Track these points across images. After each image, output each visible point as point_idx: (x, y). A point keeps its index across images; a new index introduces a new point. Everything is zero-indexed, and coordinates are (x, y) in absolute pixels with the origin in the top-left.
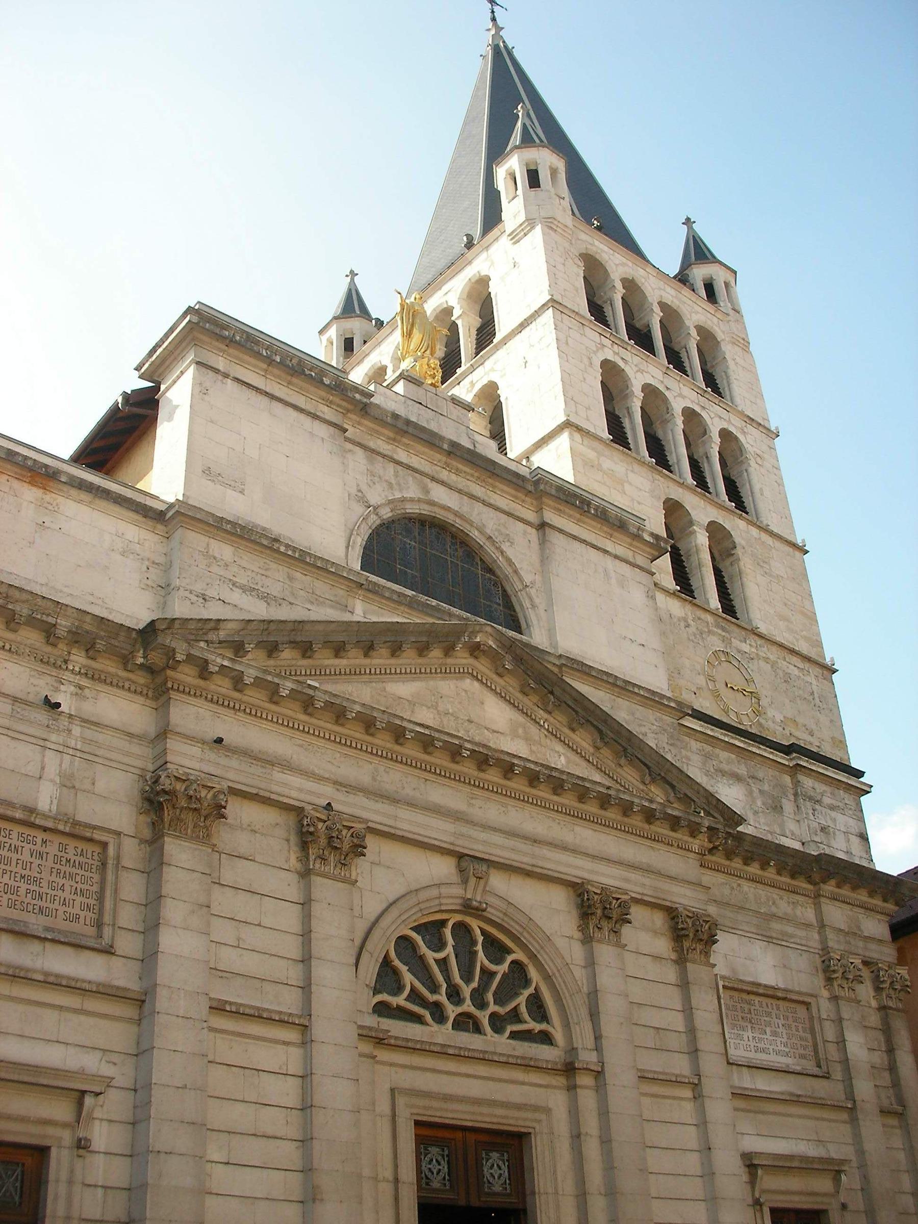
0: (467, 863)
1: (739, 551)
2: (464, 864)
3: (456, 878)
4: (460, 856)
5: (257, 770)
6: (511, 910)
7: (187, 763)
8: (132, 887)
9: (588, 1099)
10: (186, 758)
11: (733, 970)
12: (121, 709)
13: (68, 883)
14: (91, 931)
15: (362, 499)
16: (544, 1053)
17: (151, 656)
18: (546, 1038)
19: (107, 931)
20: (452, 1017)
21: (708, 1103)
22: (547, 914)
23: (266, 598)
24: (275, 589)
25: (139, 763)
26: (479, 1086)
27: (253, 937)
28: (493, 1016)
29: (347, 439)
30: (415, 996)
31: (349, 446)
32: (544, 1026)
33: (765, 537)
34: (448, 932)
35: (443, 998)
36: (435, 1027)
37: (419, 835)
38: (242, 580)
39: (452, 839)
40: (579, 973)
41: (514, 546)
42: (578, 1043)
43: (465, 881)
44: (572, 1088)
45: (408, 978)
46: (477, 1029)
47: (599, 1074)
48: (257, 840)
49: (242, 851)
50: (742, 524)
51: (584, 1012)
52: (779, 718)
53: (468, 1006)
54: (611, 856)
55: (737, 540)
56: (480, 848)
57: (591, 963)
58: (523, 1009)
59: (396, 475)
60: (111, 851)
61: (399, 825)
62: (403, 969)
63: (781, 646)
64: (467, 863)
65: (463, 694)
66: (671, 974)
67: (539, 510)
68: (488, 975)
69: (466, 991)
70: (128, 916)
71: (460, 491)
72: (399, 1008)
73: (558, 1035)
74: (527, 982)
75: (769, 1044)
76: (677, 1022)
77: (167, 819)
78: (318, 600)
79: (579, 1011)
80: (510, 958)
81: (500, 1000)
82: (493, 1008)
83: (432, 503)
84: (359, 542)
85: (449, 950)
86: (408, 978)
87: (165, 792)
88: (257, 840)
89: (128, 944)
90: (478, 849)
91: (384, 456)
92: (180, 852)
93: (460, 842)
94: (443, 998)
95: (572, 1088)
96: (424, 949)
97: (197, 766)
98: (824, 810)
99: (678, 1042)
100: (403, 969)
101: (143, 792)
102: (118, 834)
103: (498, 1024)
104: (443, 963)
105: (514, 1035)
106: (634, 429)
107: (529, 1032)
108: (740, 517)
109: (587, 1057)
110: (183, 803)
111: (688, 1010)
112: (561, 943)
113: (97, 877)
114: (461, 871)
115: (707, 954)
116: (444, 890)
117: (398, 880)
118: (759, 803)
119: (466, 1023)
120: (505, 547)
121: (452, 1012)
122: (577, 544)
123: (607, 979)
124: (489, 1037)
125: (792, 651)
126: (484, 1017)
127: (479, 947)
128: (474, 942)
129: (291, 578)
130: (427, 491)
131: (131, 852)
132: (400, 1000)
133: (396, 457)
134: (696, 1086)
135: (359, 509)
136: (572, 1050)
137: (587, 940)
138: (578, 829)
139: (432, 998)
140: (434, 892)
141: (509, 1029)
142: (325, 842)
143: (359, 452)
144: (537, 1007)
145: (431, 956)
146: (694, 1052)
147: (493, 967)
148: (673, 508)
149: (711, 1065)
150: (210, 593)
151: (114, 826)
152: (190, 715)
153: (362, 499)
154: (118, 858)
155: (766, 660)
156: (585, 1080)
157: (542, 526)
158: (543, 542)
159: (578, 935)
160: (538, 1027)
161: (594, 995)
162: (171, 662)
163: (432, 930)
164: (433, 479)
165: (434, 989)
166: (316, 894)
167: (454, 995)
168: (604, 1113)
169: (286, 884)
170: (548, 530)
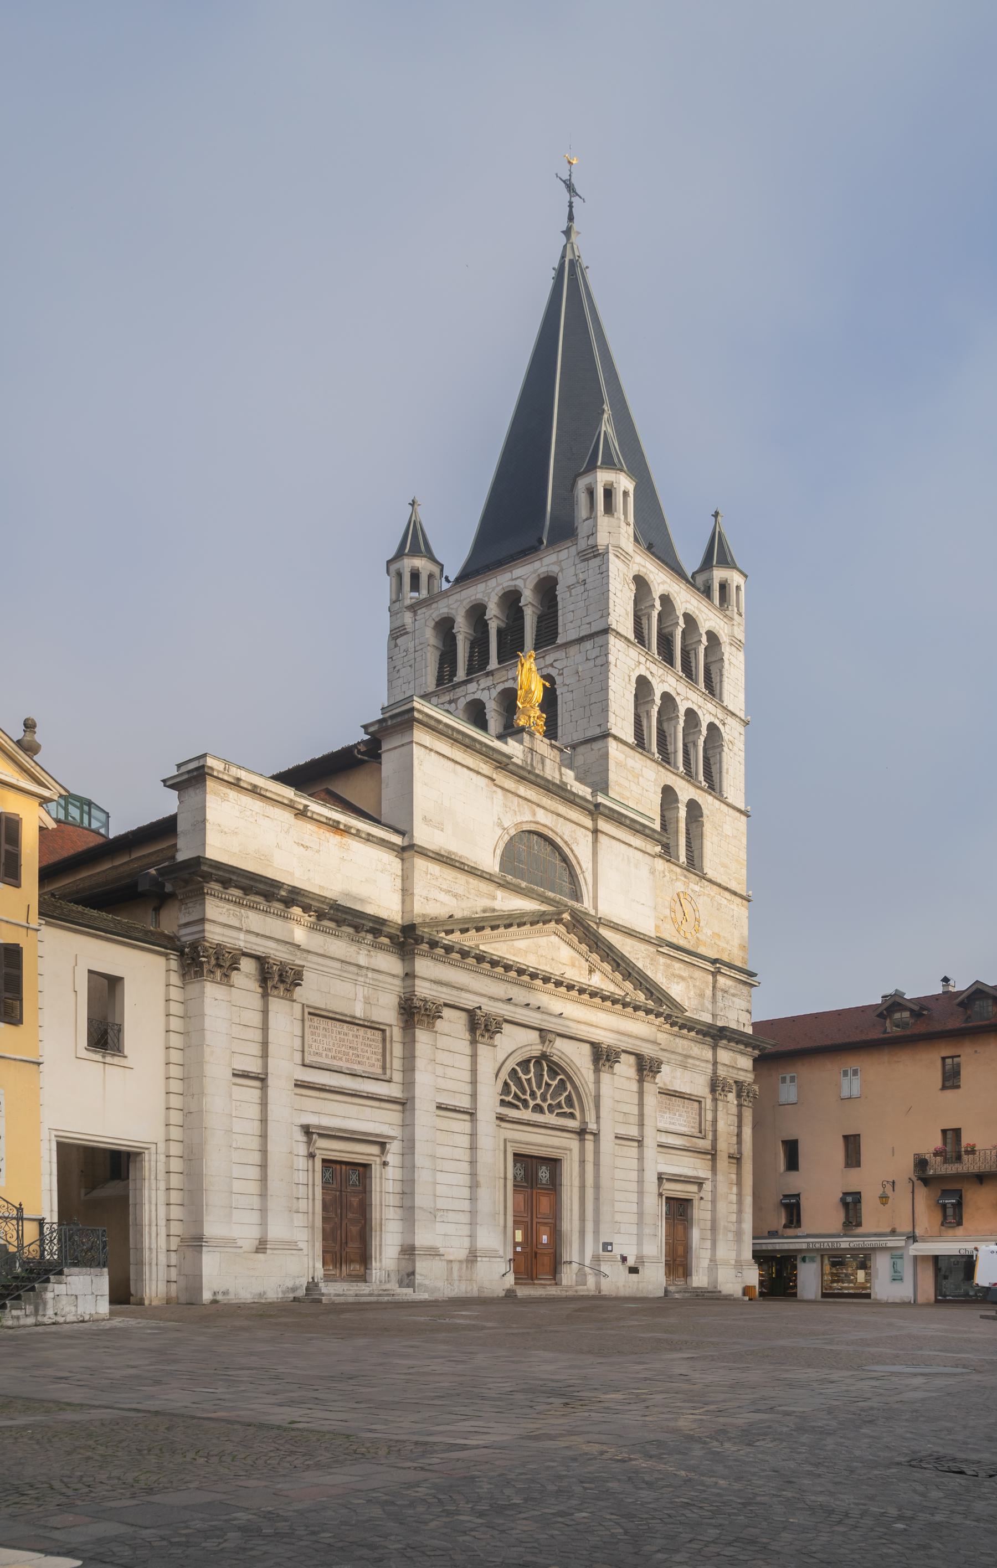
0: (543, 1033)
1: (705, 819)
2: (544, 1034)
3: (538, 1041)
4: (541, 1030)
5: (455, 992)
6: (563, 1057)
7: (424, 991)
8: (398, 1050)
9: (589, 1145)
10: (423, 990)
12: (389, 963)
14: (380, 1071)
15: (500, 824)
16: (573, 1124)
17: (407, 939)
18: (572, 1116)
19: (388, 1071)
21: (645, 1149)
22: (577, 1058)
24: (460, 890)
25: (398, 989)
26: (540, 1142)
27: (450, 1072)
28: (550, 1105)
29: (496, 785)
30: (516, 1096)
31: (495, 788)
32: (571, 1110)
33: (724, 807)
34: (532, 1065)
35: (528, 1097)
36: (524, 1111)
38: (444, 887)
39: (539, 1022)
40: (592, 1086)
41: (579, 846)
42: (587, 1120)
43: (543, 1042)
44: (582, 1140)
45: (513, 1088)
47: (596, 1135)
49: (446, 1032)
50: (710, 798)
51: (592, 1105)
53: (539, 1101)
55: (705, 811)
57: (597, 1082)
58: (563, 1102)
59: (519, 805)
60: (388, 1034)
62: (511, 1084)
64: (543, 1033)
66: (634, 1086)
67: (594, 820)
68: (548, 1085)
69: (538, 1094)
70: (397, 1064)
71: (552, 812)
73: (578, 1114)
74: (565, 1089)
75: (681, 1120)
76: (635, 1110)
77: (416, 1019)
79: (589, 1104)
80: (559, 1078)
81: (552, 1098)
82: (549, 1102)
83: (537, 823)
84: (499, 852)
85: (532, 1074)
86: (513, 1088)
87: (416, 1007)
88: (453, 1025)
89: (397, 1077)
91: (512, 793)
92: (422, 1035)
94: (528, 1097)
95: (582, 1140)
96: (521, 1074)
97: (428, 992)
99: (634, 1119)
100: (511, 1084)
101: (399, 1004)
102: (391, 1026)
104: (529, 1081)
105: (558, 1114)
106: (650, 727)
108: (710, 794)
109: (592, 1126)
110: (423, 1012)
111: (641, 1104)
112: (584, 1071)
113: (381, 1045)
114: (541, 1037)
115: (655, 1078)
116: (534, 1047)
117: (514, 1043)
119: (538, 1109)
120: (574, 847)
121: (532, 1103)
122: (614, 842)
123: (605, 1090)
126: (545, 1106)
127: (545, 1073)
128: (543, 1070)
129: (467, 882)
130: (534, 814)
131: (397, 1033)
132: (509, 1099)
133: (519, 793)
134: (640, 1142)
135: (499, 832)
136: (584, 1122)
137: (597, 1071)
139: (523, 1097)
140: (529, 1048)
142: (481, 1026)
143: (499, 790)
144: (569, 1100)
145: (523, 1077)
146: (641, 1125)
147: (550, 1082)
148: (668, 792)
149: (649, 1132)
150: (431, 896)
151: (388, 1022)
152: (423, 966)
153: (500, 824)
154: (391, 1037)
156: (588, 1137)
157: (596, 831)
158: (595, 841)
159: (592, 1067)
160: (569, 1111)
161: (597, 1098)
162: (419, 940)
163: (525, 1064)
164: (538, 805)
165: (524, 1092)
166: (479, 1052)
168: (597, 1152)
169: (463, 1046)
170: (600, 835)
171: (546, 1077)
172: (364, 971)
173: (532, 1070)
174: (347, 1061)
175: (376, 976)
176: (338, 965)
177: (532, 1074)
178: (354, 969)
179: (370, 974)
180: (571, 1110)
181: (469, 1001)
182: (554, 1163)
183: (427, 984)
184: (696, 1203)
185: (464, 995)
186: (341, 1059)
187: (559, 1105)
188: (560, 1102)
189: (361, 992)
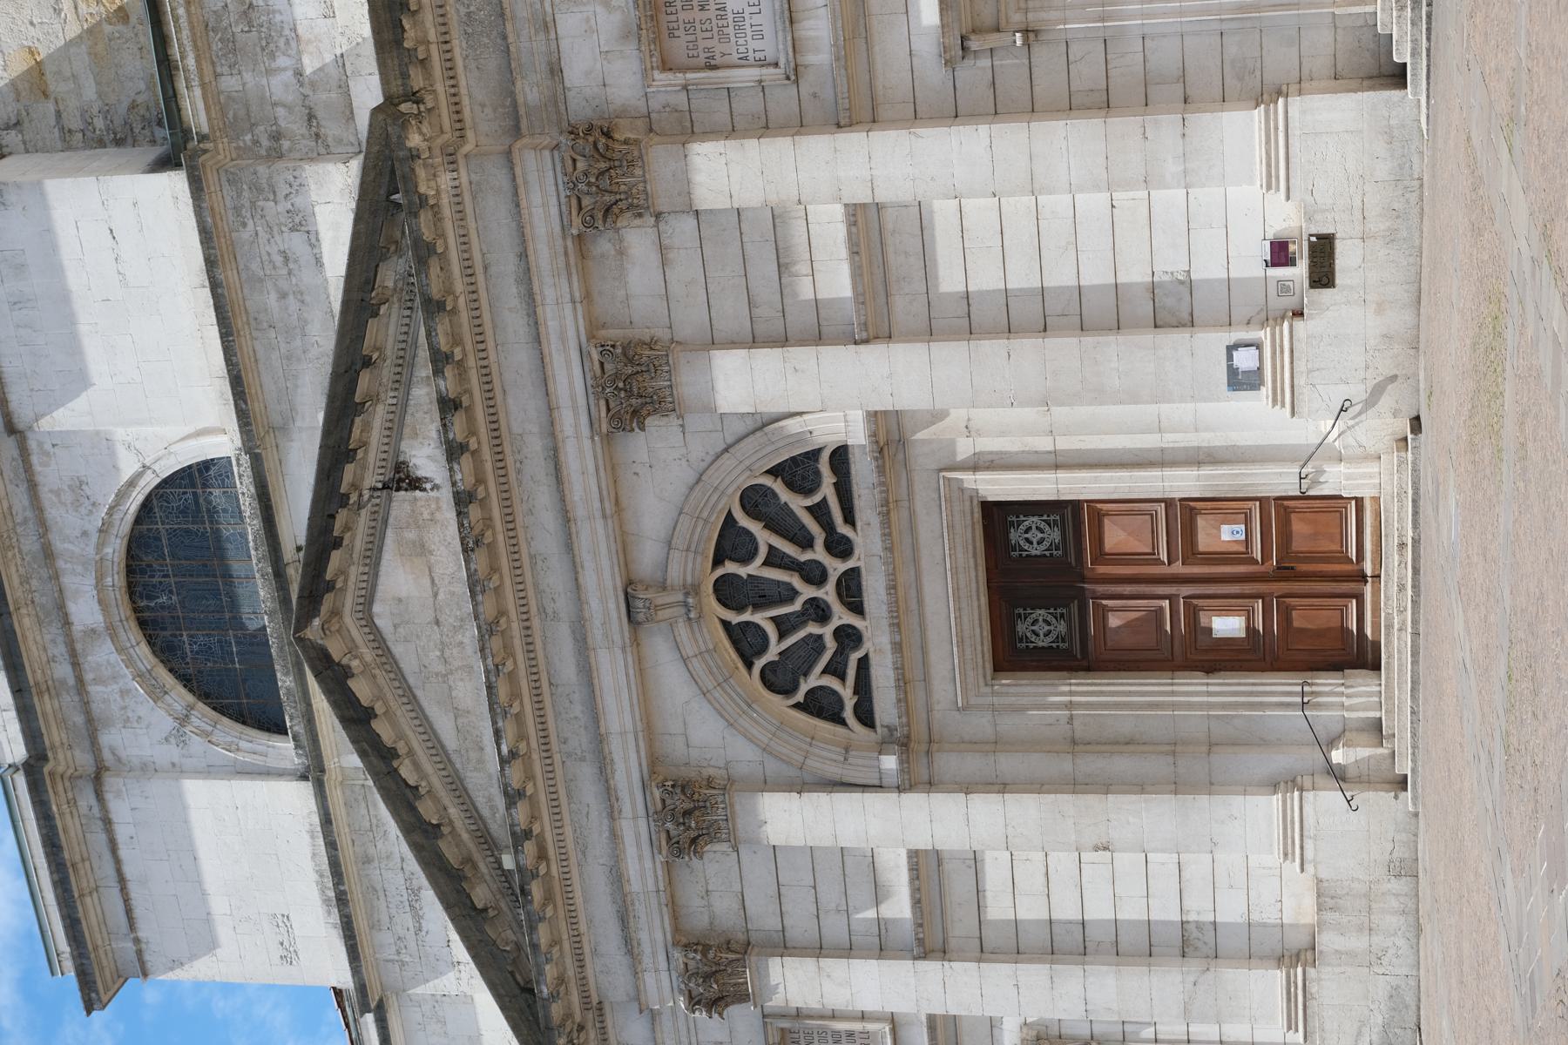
11: (625, 36)
20: (849, 619)
23: (415, 893)
35: (827, 632)
36: (867, 646)
37: (626, 666)
39: (618, 652)
48: (719, 888)
49: (736, 906)
53: (828, 593)
54: (544, 383)
56: (612, 606)
58: (809, 502)
61: (629, 726)
64: (634, 605)
65: (401, 630)
81: (806, 543)
85: (761, 618)
90: (615, 608)
93: (617, 638)
103: (840, 547)
121: (842, 616)
124: (861, 564)
126: (836, 567)
138: (516, 429)
141: (843, 529)
160: (828, 479)
167: (819, 612)
171: (754, 568)
173: (747, 617)
177: (761, 618)
181: (642, 867)
182: (1011, 655)
185: (635, 885)
187: (819, 512)
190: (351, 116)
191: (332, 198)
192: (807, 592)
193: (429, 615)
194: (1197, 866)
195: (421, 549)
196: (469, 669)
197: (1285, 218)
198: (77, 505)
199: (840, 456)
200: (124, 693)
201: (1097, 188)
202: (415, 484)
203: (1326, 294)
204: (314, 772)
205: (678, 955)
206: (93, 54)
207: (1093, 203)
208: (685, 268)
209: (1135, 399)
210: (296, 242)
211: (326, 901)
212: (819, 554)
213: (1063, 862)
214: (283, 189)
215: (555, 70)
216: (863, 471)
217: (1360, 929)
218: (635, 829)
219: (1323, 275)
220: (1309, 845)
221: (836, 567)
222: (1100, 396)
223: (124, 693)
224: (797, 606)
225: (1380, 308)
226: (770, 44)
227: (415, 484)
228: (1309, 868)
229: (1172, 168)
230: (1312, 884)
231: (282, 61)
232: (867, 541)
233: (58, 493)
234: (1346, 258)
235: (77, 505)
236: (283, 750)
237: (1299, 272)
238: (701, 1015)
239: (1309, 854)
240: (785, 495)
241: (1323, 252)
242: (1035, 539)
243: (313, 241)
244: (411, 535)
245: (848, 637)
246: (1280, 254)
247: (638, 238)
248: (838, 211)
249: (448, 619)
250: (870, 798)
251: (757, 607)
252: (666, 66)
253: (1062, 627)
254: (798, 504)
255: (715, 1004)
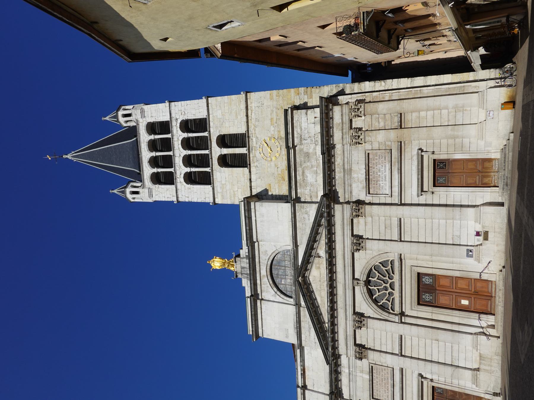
5: (348, 338)
6: (363, 273)
11: (363, 188)
13: (381, 373)
20: (391, 291)
23: (310, 328)
27: (384, 341)
35: (387, 292)
36: (395, 296)
46: (393, 282)
48: (362, 337)
52: (272, 128)
53: (388, 285)
63: (247, 122)
72: (392, 304)
73: (391, 259)
78: (305, 315)
98: (303, 134)
105: (394, 274)
107: (391, 267)
118: (309, 164)
119: (392, 286)
121: (390, 290)
125: (247, 116)
126: (390, 281)
144: (384, 264)
155: (255, 131)
160: (390, 265)
167: (386, 289)
172: (351, 372)
174: (388, 384)
175: (351, 367)
176: (351, 383)
178: (351, 376)
179: (351, 370)
180: (389, 263)
183: (349, 351)
184: (436, 157)
185: (348, 333)
186: (388, 387)
188: (389, 301)
189: (359, 374)
190: (317, 197)
191: (312, 211)
192: (385, 285)
193: (319, 280)
194: (456, 347)
195: (319, 268)
196: (324, 290)
197: (479, 228)
198: (265, 255)
199: (392, 262)
200: (267, 287)
201: (443, 219)
202: (319, 257)
203: (486, 241)
204: (298, 305)
205: (354, 347)
206: (279, 186)
207: (442, 222)
208: (369, 226)
209: (448, 257)
210: (306, 216)
211: (295, 328)
212: (387, 278)
213: (428, 342)
214: (305, 207)
215: (351, 192)
216: (397, 264)
217: (489, 365)
218: (350, 323)
219: (486, 238)
220: (479, 346)
221: (390, 281)
222: (442, 256)
223: (267, 287)
224: (382, 287)
225: (497, 245)
226: (388, 191)
227: (319, 257)
228: (479, 351)
229: (458, 217)
230: (479, 354)
231: (308, 188)
232: (396, 277)
233: (262, 252)
234: (490, 236)
235: (265, 255)
236: (292, 301)
237: (481, 238)
238: (357, 361)
239: (479, 348)
240: (382, 267)
241: (486, 234)
242: (427, 280)
243: (309, 216)
244: (318, 265)
245: (391, 294)
246: (478, 234)
247: (361, 220)
248: (397, 219)
249: (322, 281)
250: (393, 323)
251: (375, 286)
252: (369, 193)
253: (431, 298)
254: (384, 269)
255: (361, 359)
